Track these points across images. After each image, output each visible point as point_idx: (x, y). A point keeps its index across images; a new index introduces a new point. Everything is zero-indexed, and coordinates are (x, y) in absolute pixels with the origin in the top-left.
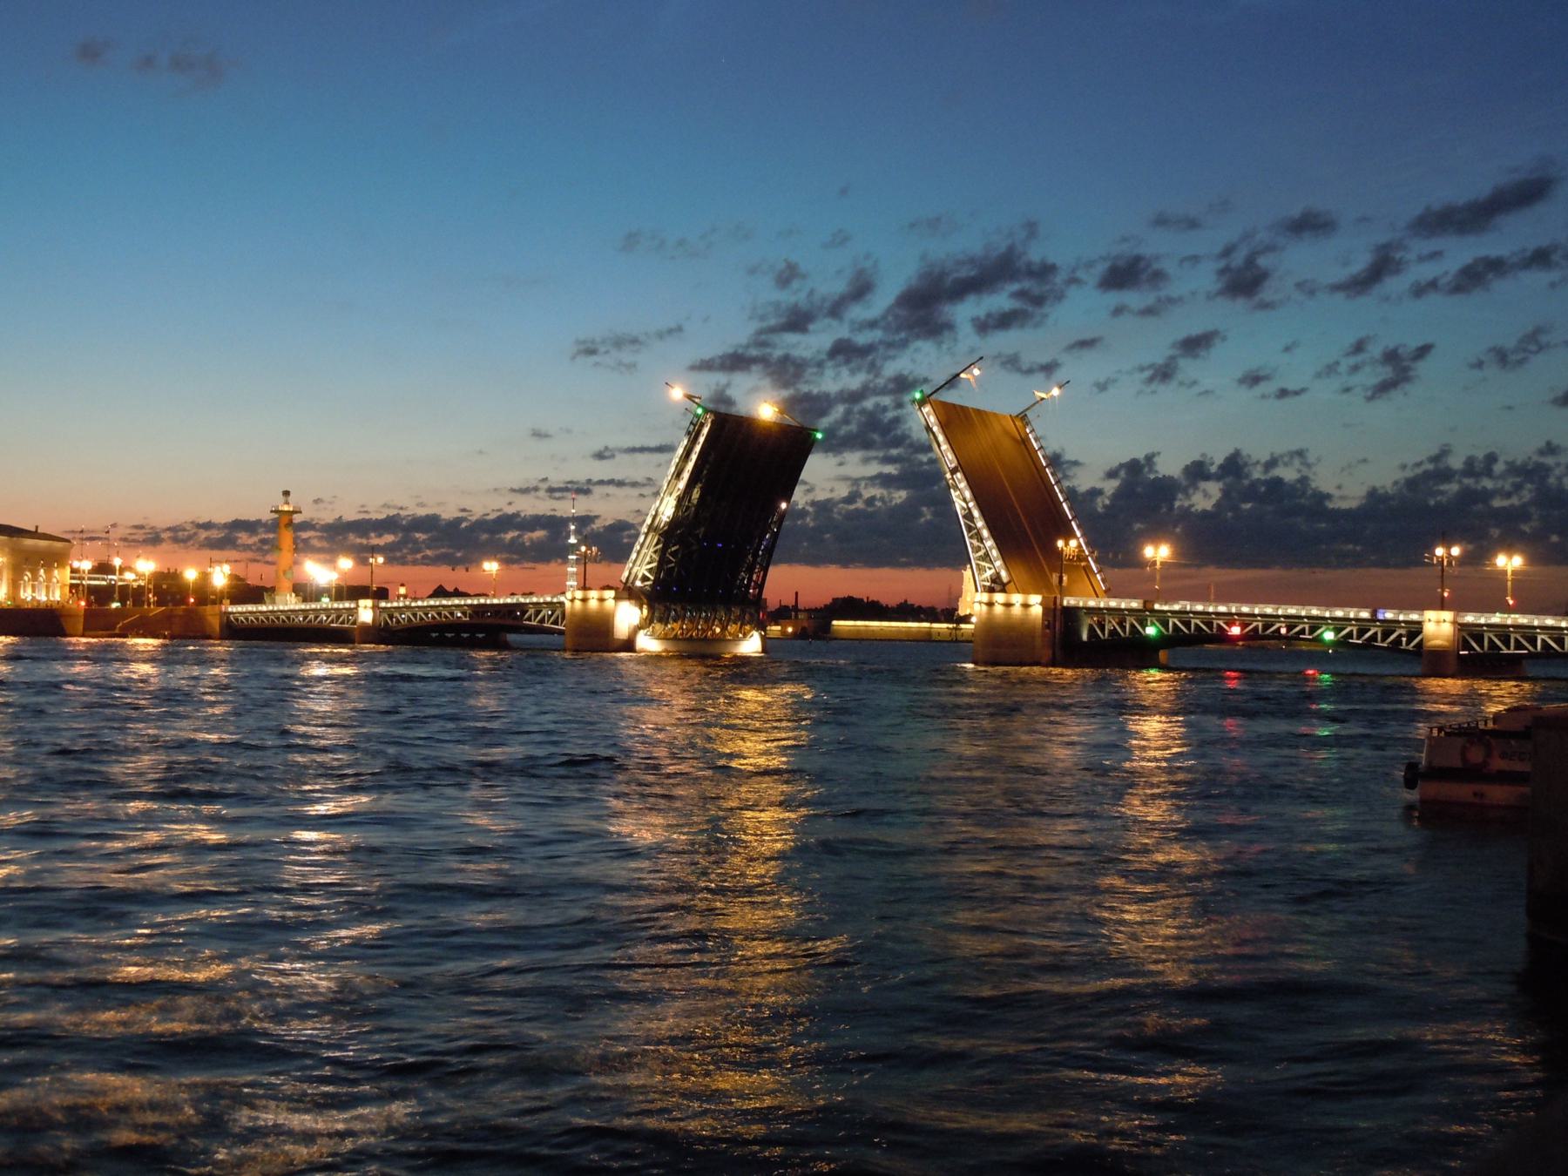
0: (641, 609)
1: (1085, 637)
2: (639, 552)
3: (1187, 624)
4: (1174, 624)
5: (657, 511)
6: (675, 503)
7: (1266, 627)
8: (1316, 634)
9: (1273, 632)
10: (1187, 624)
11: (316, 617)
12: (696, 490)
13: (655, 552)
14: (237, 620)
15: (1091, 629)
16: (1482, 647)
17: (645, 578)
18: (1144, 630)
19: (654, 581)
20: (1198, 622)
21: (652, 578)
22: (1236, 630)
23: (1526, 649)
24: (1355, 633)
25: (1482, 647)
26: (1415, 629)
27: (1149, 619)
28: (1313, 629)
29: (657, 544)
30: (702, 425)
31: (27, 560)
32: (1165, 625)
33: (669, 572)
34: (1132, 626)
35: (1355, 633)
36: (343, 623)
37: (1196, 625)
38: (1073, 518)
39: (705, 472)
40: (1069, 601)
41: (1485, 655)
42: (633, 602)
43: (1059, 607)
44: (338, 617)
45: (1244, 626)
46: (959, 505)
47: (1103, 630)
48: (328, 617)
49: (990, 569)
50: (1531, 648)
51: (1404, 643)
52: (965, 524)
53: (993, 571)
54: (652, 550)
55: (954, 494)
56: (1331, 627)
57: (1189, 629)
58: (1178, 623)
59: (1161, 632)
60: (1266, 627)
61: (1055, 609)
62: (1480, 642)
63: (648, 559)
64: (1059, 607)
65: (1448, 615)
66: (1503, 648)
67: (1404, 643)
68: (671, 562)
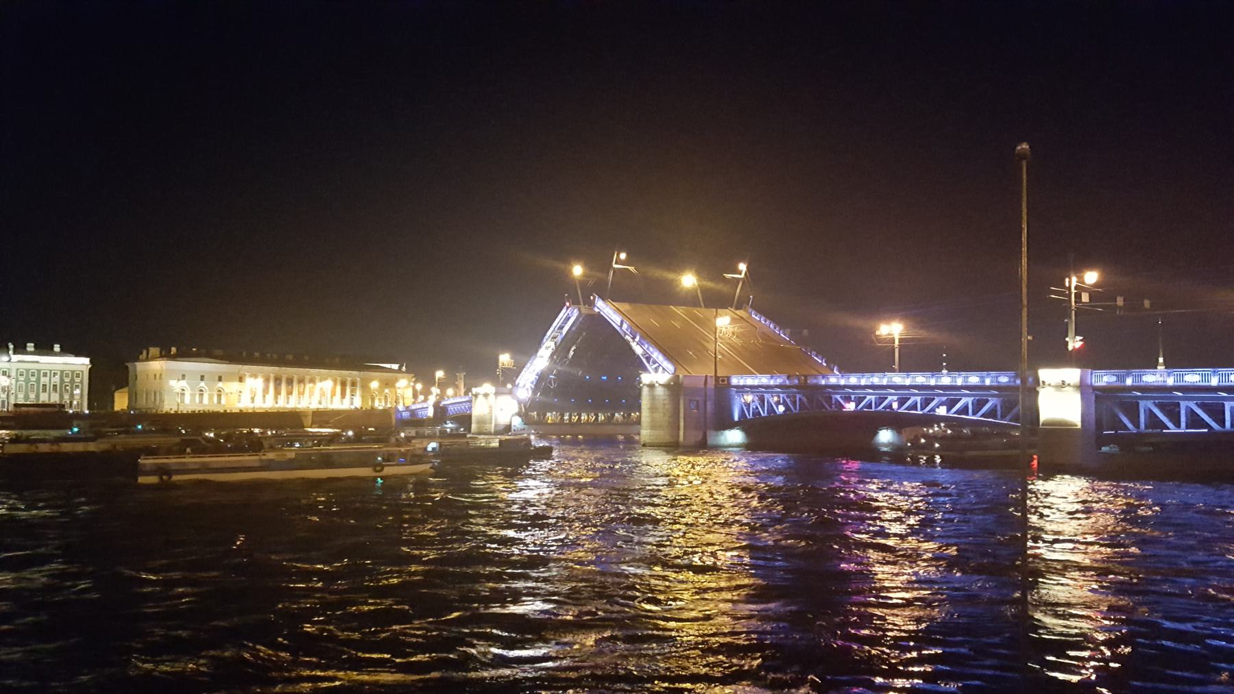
1: (736, 418)
8: (928, 408)
18: (778, 409)
22: (850, 406)
23: (1207, 426)
25: (1136, 424)
28: (926, 402)
45: (859, 401)
56: (944, 399)
65: (1072, 375)
66: (1170, 425)
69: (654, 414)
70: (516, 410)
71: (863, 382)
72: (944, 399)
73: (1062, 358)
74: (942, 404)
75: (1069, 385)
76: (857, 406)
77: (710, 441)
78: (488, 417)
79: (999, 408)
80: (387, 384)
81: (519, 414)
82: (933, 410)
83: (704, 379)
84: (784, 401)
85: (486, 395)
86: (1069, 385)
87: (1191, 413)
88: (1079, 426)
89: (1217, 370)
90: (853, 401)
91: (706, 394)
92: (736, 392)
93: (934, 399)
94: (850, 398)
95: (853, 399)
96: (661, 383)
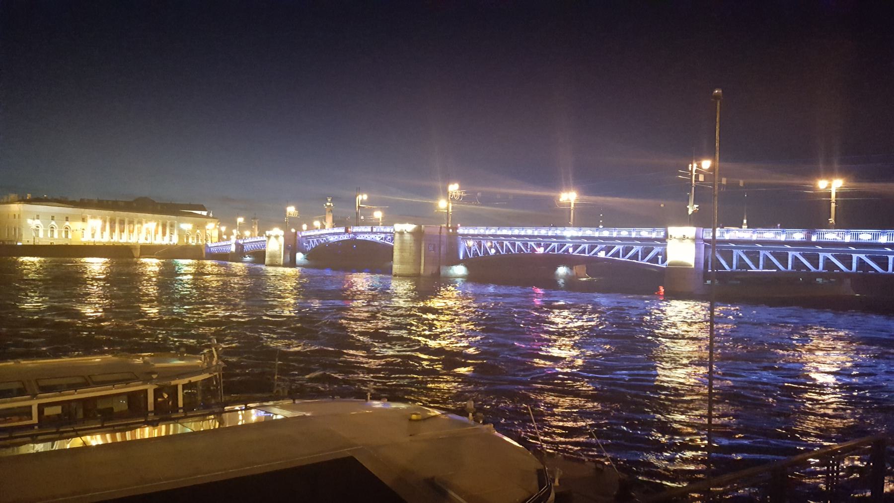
1: (461, 257)
8: (593, 253)
18: (491, 251)
22: (540, 250)
24: (621, 251)
28: (592, 248)
31: (198, 226)
35: (621, 251)
41: (732, 273)
45: (546, 246)
50: (781, 267)
58: (509, 245)
59: (497, 251)
65: (691, 231)
66: (752, 266)
69: (403, 254)
71: (550, 233)
72: (604, 246)
73: (683, 219)
74: (602, 250)
75: (688, 238)
78: (278, 253)
79: (640, 254)
80: (198, 226)
82: (596, 253)
83: (439, 229)
84: (495, 246)
85: (277, 237)
86: (688, 238)
87: (767, 258)
88: (693, 266)
89: (785, 230)
90: (542, 247)
91: (440, 241)
92: (462, 239)
93: (597, 246)
94: (541, 244)
95: (542, 245)
96: (408, 231)
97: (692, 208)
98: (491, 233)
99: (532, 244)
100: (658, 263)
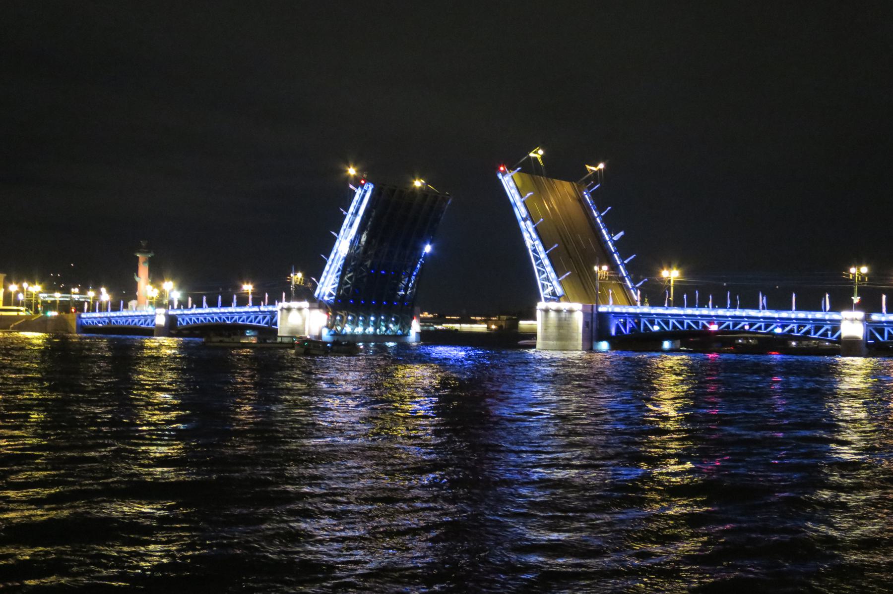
0: (327, 313)
2: (326, 277)
3: (682, 323)
4: (673, 323)
5: (337, 250)
6: (348, 244)
7: (735, 325)
9: (740, 328)
10: (682, 323)
11: (133, 321)
12: (364, 236)
13: (337, 277)
14: (87, 322)
15: (618, 328)
16: (883, 337)
17: (330, 295)
18: (653, 328)
19: (335, 296)
20: (689, 321)
21: (334, 294)
22: (714, 328)
26: (835, 326)
27: (656, 320)
28: (767, 326)
29: (338, 271)
30: (366, 192)
32: (667, 323)
33: (347, 290)
34: (645, 325)
36: (148, 325)
37: (688, 323)
38: (616, 251)
39: (369, 223)
40: (602, 309)
42: (322, 310)
43: (595, 312)
44: (146, 321)
45: (720, 324)
46: (529, 243)
47: (625, 329)
48: (139, 321)
49: (550, 286)
51: (829, 335)
52: (534, 256)
53: (552, 288)
54: (335, 275)
55: (526, 236)
56: (779, 324)
57: (683, 326)
59: (662, 328)
60: (735, 325)
61: (592, 314)
62: (881, 333)
63: (332, 282)
64: (595, 312)
67: (829, 335)
68: (347, 283)
69: (561, 331)
70: (325, 323)
72: (779, 324)
73: (849, 306)
76: (719, 327)
77: (594, 348)
81: (327, 326)
82: (772, 330)
83: (590, 307)
88: (862, 338)
97: (856, 300)
98: (831, 318)
99: (704, 322)
100: (828, 337)
